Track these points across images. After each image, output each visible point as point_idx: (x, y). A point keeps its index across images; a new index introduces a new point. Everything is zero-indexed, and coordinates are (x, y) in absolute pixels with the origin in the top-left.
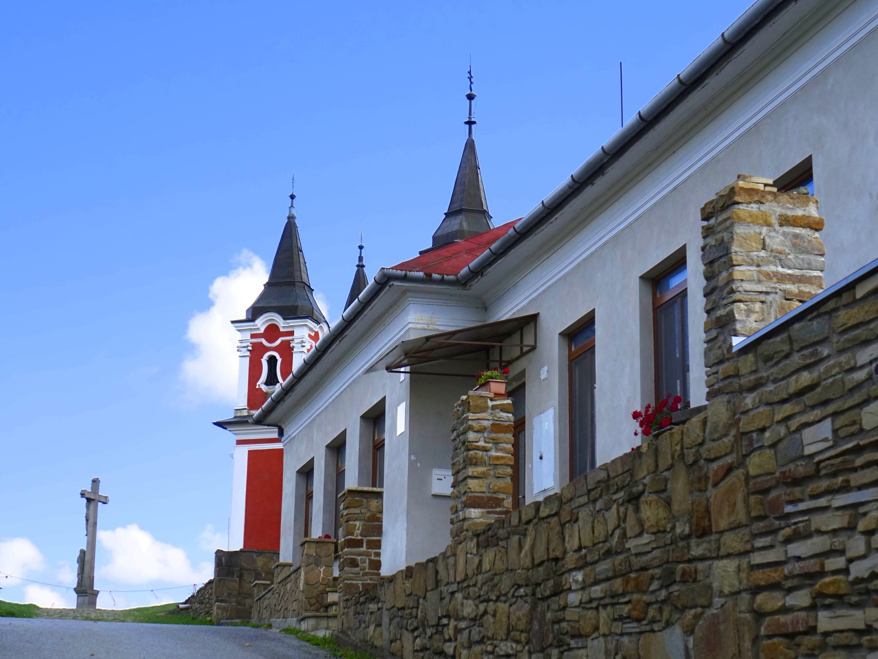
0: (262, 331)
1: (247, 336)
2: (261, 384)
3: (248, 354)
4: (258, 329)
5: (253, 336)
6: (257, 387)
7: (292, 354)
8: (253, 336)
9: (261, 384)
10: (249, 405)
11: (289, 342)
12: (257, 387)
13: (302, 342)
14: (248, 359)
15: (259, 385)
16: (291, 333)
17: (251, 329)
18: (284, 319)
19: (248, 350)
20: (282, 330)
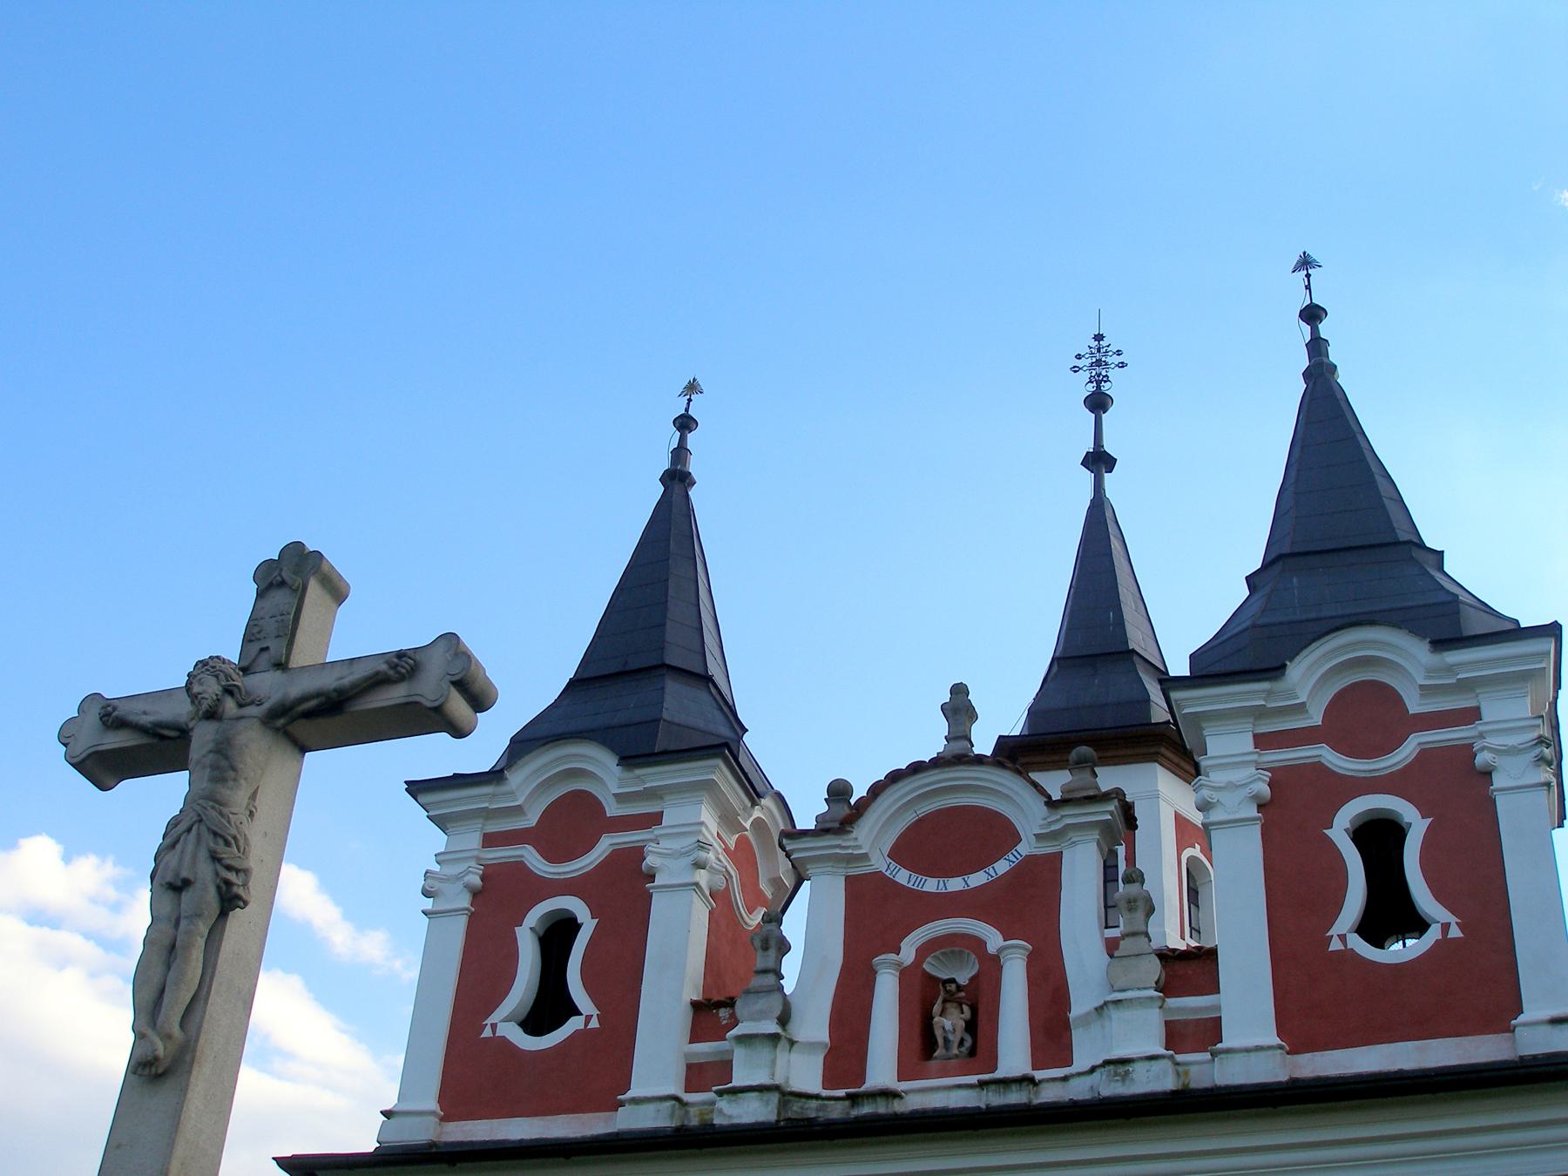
0: (531, 819)
1: (471, 840)
2: (504, 1023)
3: (465, 901)
4: (518, 810)
5: (490, 840)
6: (487, 1033)
7: (648, 898)
8: (490, 840)
9: (504, 1023)
10: (441, 1099)
11: (638, 853)
12: (487, 1033)
13: (702, 846)
14: (462, 922)
17: (488, 814)
18: (629, 760)
19: (466, 886)
20: (612, 810)
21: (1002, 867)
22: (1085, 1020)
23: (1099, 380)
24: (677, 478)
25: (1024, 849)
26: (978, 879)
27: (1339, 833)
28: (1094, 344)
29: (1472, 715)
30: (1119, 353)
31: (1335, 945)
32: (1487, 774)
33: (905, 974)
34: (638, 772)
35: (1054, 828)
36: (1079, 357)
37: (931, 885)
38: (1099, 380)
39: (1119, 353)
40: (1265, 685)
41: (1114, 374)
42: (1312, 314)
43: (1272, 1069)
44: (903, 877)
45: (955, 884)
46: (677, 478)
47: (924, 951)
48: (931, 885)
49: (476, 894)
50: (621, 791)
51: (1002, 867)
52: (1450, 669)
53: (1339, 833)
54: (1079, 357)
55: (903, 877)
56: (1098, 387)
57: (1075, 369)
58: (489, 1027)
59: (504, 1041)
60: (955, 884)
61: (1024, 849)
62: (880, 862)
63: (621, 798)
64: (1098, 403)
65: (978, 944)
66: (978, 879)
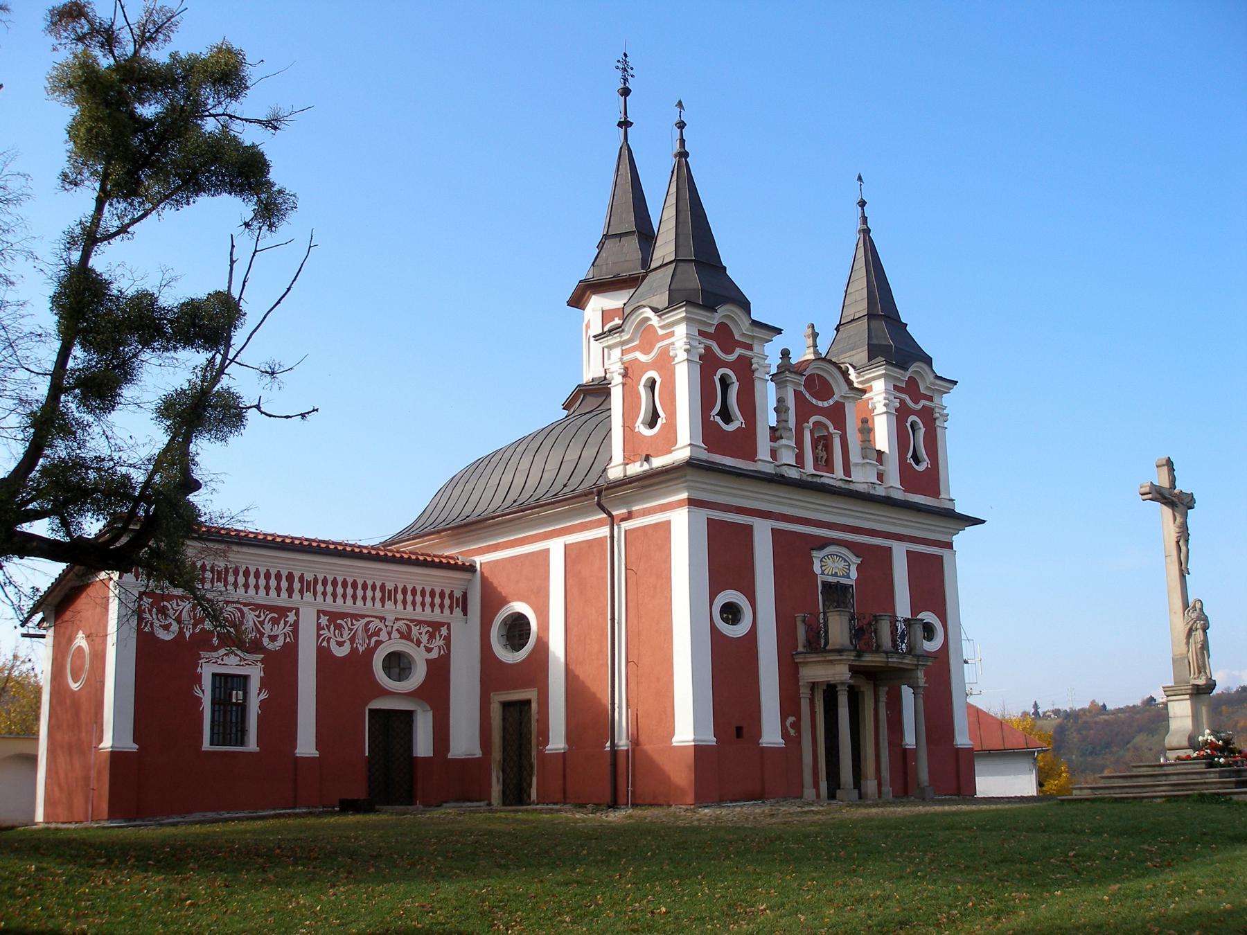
12: (712, 419)
15: (714, 416)
16: (750, 347)
20: (737, 337)
21: (831, 402)
22: (857, 464)
23: (626, 80)
24: (683, 154)
25: (836, 397)
26: (826, 404)
27: (908, 425)
28: (624, 58)
29: (931, 399)
30: (632, 69)
31: (909, 461)
32: (935, 419)
33: (812, 432)
34: (755, 329)
35: (847, 395)
36: (619, 61)
37: (814, 401)
38: (626, 80)
39: (632, 69)
40: (902, 372)
41: (629, 78)
42: (862, 204)
43: (899, 495)
44: (807, 396)
45: (820, 404)
46: (683, 154)
47: (816, 424)
48: (814, 401)
49: (701, 357)
50: (745, 332)
51: (831, 402)
52: (934, 384)
53: (908, 425)
54: (619, 61)
55: (807, 396)
56: (625, 84)
57: (617, 68)
58: (712, 417)
59: (717, 422)
60: (820, 404)
61: (836, 397)
62: (802, 389)
63: (743, 335)
64: (626, 92)
65: (827, 429)
66: (826, 404)
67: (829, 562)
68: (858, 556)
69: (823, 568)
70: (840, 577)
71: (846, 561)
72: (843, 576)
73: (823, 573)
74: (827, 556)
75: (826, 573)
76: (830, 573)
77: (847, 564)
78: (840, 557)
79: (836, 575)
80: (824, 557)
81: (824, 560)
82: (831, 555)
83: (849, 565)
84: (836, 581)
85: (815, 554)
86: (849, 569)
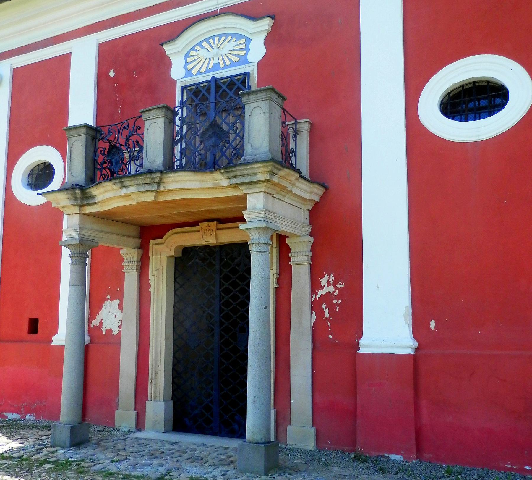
67: (202, 53)
68: (254, 18)
69: (190, 66)
70: (226, 67)
71: (239, 36)
72: (233, 64)
73: (189, 73)
74: (200, 44)
75: (194, 72)
76: (203, 69)
77: (244, 40)
78: (227, 35)
79: (216, 67)
80: (193, 49)
81: (192, 53)
82: (207, 40)
83: (248, 40)
84: (209, 78)
85: (168, 49)
86: (247, 49)
